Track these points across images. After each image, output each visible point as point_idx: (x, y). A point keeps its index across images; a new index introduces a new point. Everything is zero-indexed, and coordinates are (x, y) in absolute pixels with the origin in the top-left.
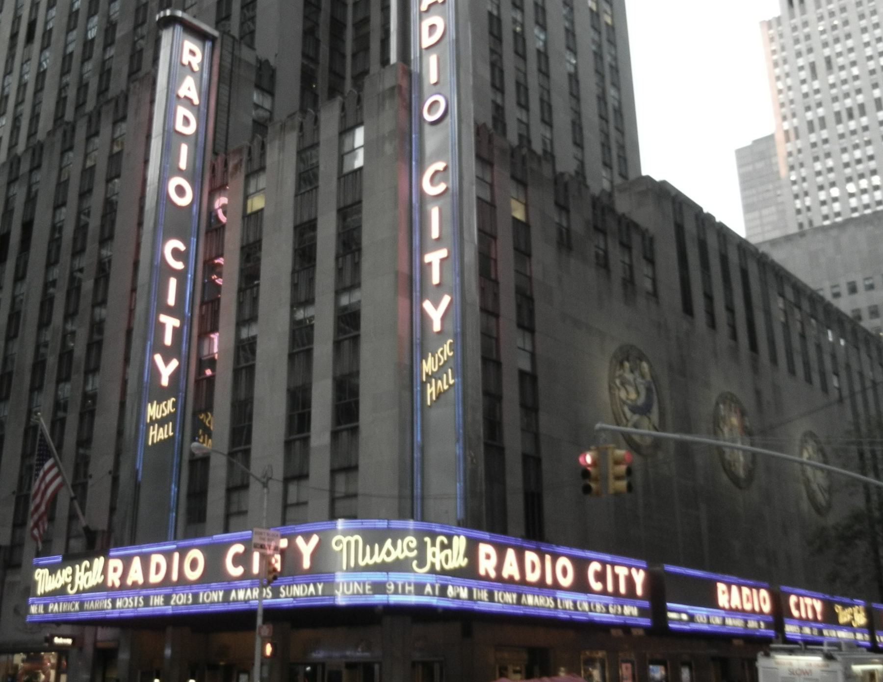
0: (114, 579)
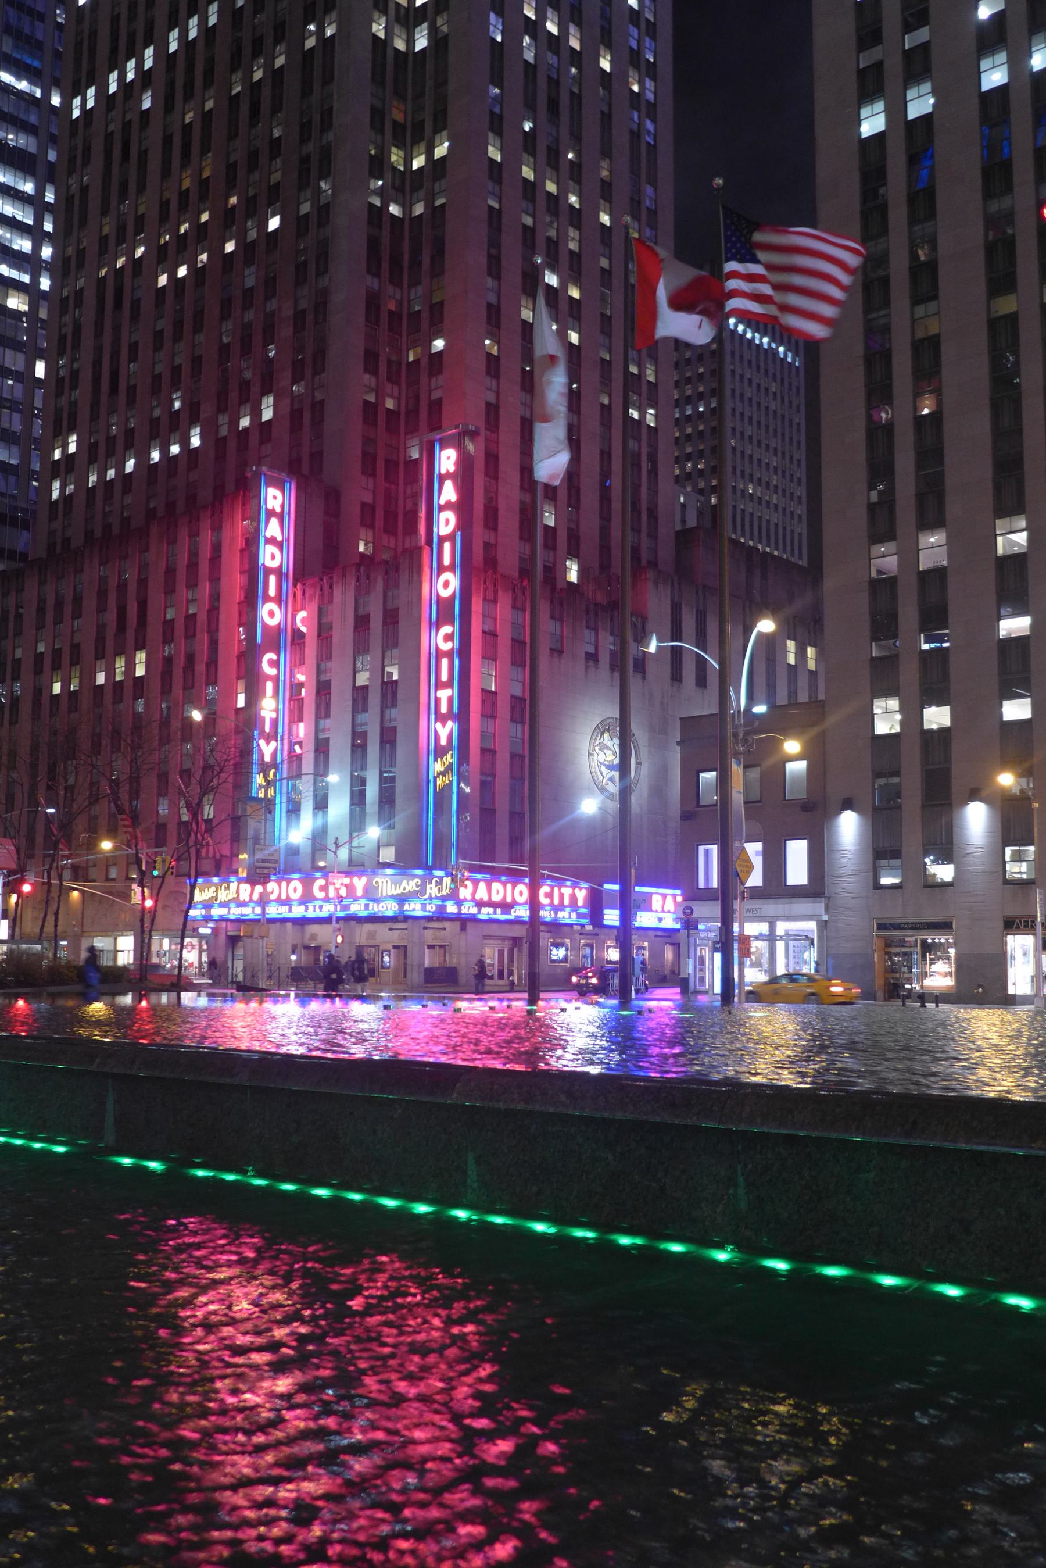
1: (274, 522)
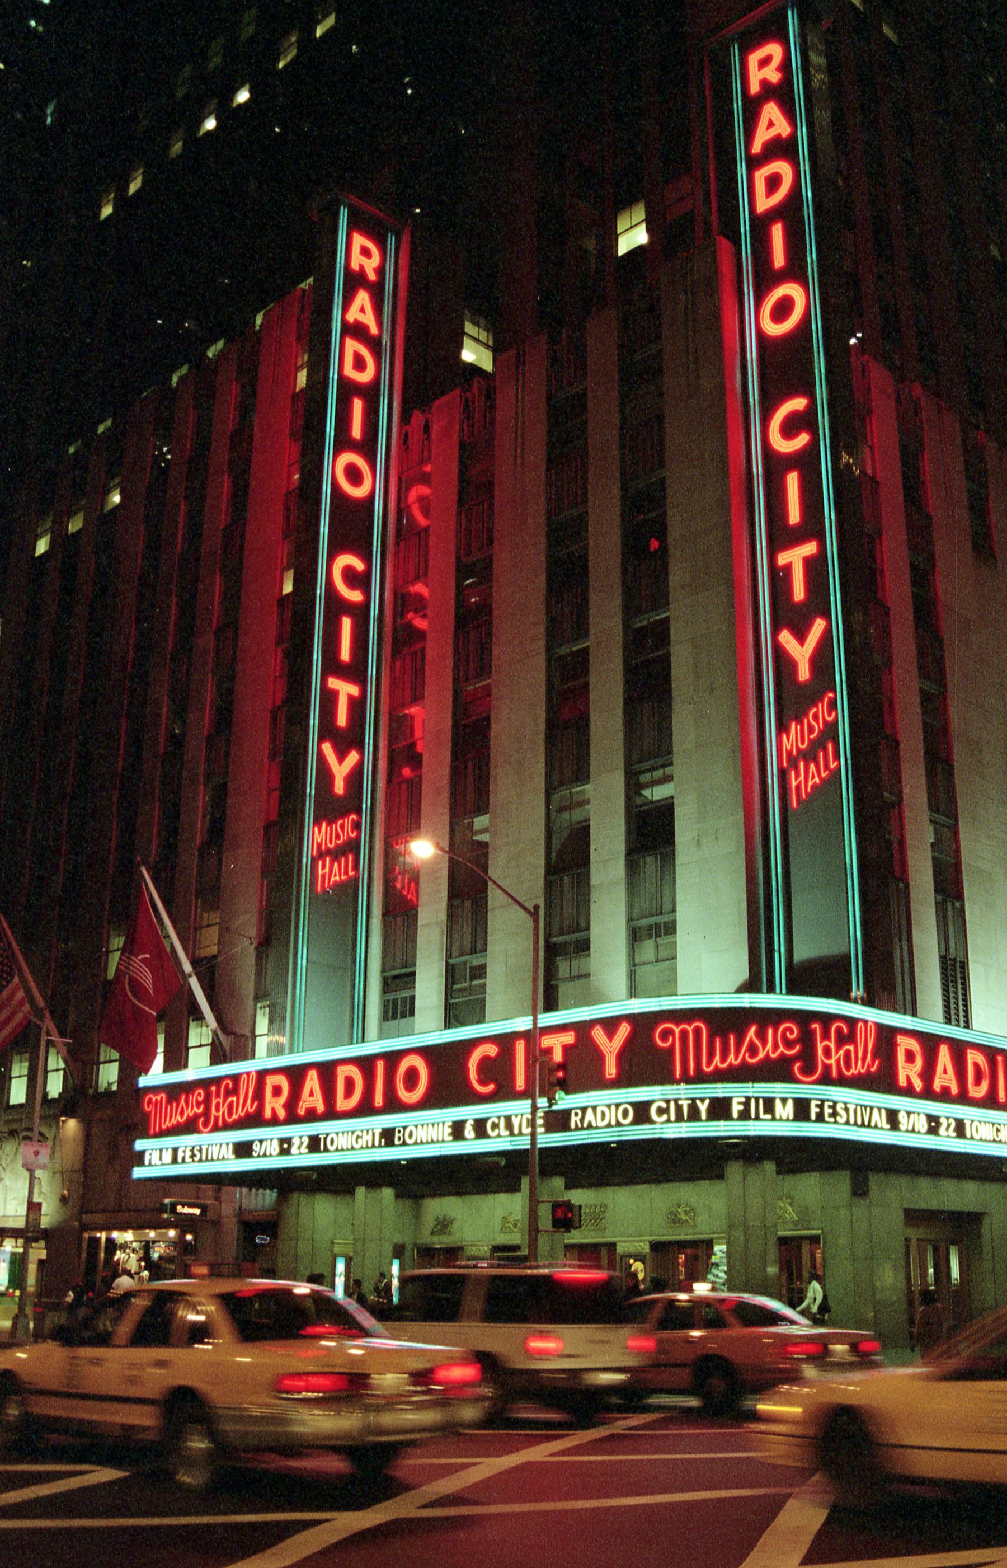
0: (275, 1105)
1: (362, 298)
